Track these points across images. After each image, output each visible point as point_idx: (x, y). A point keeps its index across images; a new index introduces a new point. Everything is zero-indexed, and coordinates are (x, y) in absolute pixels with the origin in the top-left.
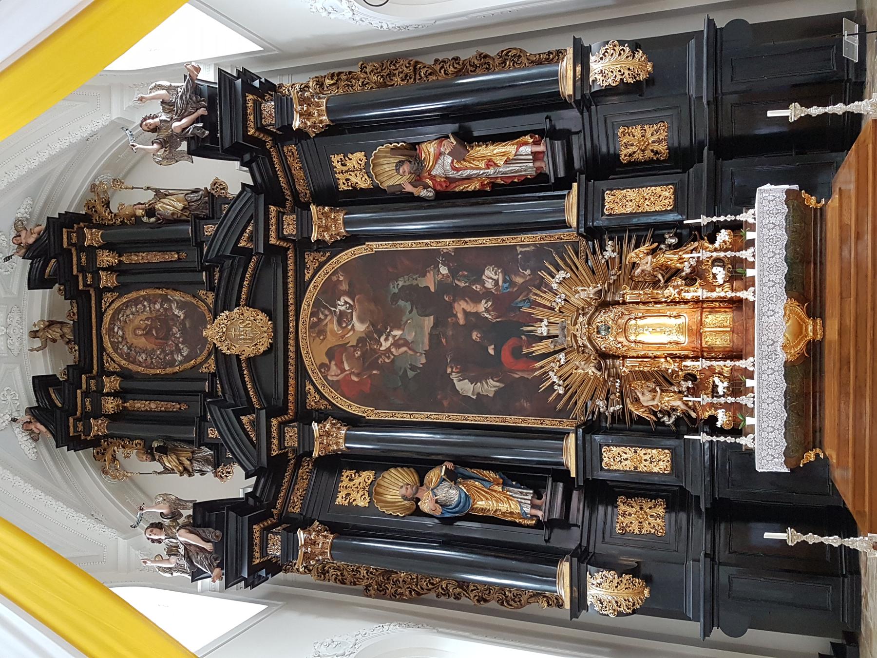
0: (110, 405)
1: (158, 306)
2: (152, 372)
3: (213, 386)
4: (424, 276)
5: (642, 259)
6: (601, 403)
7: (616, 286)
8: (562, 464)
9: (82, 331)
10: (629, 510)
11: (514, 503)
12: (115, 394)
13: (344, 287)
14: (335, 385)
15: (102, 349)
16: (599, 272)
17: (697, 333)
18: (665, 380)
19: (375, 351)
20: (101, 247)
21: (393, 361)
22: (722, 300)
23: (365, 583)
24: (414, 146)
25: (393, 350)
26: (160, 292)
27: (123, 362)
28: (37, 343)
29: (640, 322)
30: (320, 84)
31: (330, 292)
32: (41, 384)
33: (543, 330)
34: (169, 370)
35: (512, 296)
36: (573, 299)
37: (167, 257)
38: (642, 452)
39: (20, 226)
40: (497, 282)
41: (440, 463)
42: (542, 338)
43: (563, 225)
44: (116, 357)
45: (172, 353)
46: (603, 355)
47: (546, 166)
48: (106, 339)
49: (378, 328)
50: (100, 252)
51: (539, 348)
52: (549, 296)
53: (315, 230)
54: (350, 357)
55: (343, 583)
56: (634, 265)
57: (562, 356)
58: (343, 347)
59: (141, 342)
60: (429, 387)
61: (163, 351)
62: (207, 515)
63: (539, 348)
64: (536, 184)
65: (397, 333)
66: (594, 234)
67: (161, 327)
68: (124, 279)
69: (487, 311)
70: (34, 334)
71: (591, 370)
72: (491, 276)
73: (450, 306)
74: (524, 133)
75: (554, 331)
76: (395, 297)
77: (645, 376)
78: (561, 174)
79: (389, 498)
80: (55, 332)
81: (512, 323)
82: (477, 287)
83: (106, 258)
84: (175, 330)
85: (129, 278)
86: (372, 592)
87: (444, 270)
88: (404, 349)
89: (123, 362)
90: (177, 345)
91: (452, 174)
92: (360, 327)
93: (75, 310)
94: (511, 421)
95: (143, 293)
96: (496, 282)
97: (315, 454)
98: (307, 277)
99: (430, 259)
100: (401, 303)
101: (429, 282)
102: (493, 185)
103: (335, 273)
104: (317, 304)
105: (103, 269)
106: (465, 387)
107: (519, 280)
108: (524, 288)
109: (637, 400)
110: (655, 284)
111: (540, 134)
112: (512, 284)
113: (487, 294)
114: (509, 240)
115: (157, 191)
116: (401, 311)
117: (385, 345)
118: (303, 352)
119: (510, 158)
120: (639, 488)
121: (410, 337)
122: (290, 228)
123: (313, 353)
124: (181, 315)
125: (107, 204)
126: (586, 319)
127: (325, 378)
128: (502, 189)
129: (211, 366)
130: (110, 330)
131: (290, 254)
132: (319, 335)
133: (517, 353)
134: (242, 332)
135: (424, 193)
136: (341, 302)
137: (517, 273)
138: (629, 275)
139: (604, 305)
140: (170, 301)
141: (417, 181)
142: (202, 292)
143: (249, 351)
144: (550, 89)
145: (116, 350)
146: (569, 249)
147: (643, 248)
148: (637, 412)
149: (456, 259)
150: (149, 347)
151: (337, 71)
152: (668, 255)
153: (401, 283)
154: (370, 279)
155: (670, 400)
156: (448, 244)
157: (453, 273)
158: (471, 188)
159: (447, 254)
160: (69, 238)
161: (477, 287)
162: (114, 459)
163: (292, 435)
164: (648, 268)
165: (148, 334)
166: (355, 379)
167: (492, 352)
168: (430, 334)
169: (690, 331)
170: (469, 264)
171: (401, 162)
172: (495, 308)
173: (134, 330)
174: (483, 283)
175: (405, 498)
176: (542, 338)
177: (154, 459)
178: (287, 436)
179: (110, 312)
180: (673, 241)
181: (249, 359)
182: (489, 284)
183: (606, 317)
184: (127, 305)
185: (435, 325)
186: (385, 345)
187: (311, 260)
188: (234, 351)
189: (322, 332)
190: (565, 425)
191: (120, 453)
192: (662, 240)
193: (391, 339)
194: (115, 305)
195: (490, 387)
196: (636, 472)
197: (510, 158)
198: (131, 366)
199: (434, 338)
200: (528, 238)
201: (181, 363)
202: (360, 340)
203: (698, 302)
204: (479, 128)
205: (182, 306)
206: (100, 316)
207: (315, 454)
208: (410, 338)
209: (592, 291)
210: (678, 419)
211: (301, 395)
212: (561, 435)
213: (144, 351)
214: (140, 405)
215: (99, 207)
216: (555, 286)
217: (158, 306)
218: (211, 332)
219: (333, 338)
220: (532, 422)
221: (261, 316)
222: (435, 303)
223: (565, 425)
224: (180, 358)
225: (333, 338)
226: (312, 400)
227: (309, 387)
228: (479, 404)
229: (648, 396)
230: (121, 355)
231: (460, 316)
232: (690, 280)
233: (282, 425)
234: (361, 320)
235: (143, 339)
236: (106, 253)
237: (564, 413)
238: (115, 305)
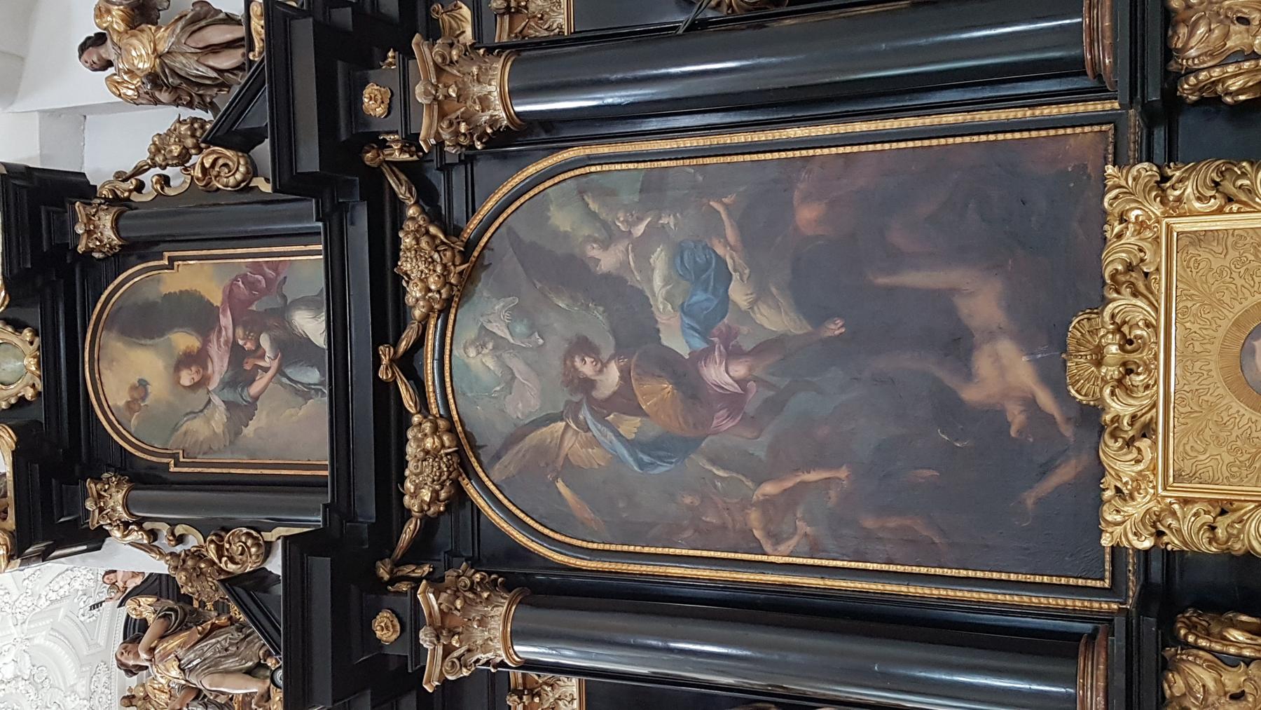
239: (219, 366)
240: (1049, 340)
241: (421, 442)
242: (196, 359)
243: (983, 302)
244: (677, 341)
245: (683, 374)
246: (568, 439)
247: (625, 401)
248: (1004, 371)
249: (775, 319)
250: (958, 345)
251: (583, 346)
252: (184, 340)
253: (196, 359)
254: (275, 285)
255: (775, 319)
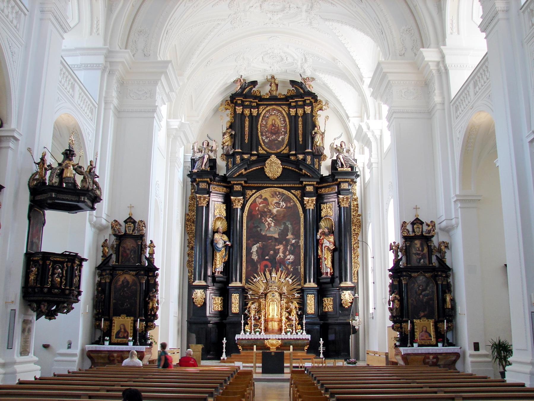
0: (247, 112)
1: (283, 130)
2: (259, 127)
3: (254, 155)
4: (292, 234)
5: (294, 305)
6: (251, 292)
7: (287, 298)
8: (232, 281)
9: (273, 99)
10: (219, 300)
11: (219, 267)
12: (251, 114)
13: (289, 205)
14: (255, 201)
15: (268, 105)
16: (291, 292)
17: (272, 320)
18: (259, 311)
19: (267, 216)
20: (304, 111)
21: (263, 223)
22: (281, 326)
23: (190, 214)
24: (333, 233)
25: (267, 223)
26: (288, 130)
27: (262, 115)
28: (269, 77)
29: (275, 305)
30: (356, 200)
31: (287, 200)
32: (254, 83)
33: (274, 275)
34: (259, 134)
35: (285, 265)
36: (283, 284)
37: (300, 136)
38: (238, 305)
39: (313, 79)
40: (289, 259)
41: (230, 241)
42: (271, 274)
43: (305, 282)
44: (264, 111)
45: (266, 135)
46: (266, 295)
47: (324, 276)
48: (271, 107)
49: (275, 218)
50: (302, 110)
51: (268, 274)
52: (284, 277)
53: (307, 198)
54: (264, 207)
55: (189, 206)
56: (292, 302)
57: (265, 281)
58: (268, 204)
59: (270, 122)
60: (255, 236)
61: (267, 131)
62: (212, 162)
63: (268, 274)
64: (318, 272)
65: (273, 224)
66: (302, 291)
67: (275, 131)
68: (293, 118)
69: (280, 256)
70: (273, 77)
71: (261, 291)
72: (291, 258)
73: (281, 243)
74: (334, 270)
75: (273, 279)
76: (285, 224)
77: (260, 305)
78: (321, 281)
79: (217, 222)
80: (274, 88)
81: (276, 264)
82: (287, 253)
83: (300, 112)
84: (274, 136)
85: (294, 119)
86: (188, 217)
87: (293, 241)
88: (267, 227)
89: (262, 115)
90: (268, 137)
91: (324, 245)
92: (275, 211)
93: (282, 97)
94: (244, 264)
95: (288, 123)
96: (289, 259)
97: (232, 198)
98: (292, 191)
99: (297, 237)
100: (283, 226)
101: (290, 236)
102: (320, 258)
103: (294, 202)
104: (283, 194)
105: (296, 110)
106: (255, 248)
107: (289, 267)
108: (287, 269)
109: (253, 303)
110: (287, 308)
111: (333, 275)
112: (288, 264)
113: (285, 256)
114: (302, 264)
115: (323, 133)
116: (280, 226)
117: (269, 220)
118: (266, 189)
119: (327, 266)
120: (226, 303)
121: (272, 229)
122: (309, 189)
123: (266, 193)
124: (280, 139)
125: (321, 109)
126: (276, 290)
127: (257, 197)
128: (318, 261)
129: (261, 152)
130: (274, 109)
131: (300, 185)
132: (272, 195)
133: (266, 266)
134: (274, 167)
135: (318, 236)
136: (284, 204)
137: (292, 266)
138: (289, 301)
139: (281, 295)
140: (285, 135)
141: (323, 234)
142: (288, 148)
143: (267, 170)
144: (343, 280)
145: (267, 111)
146: (299, 283)
147: (297, 306)
148: (249, 305)
149: (296, 246)
150: (268, 126)
151: (359, 206)
152: (295, 312)
153: (289, 226)
154: (290, 214)
155: (253, 313)
156: (302, 243)
157: (292, 245)
158: (319, 252)
159: (298, 242)
160: (308, 99)
161: (287, 253)
162: (227, 109)
163: (238, 188)
164: (291, 307)
165: (273, 125)
166: (257, 208)
167: (266, 258)
168: (272, 237)
169: (273, 318)
170: (295, 250)
171: (328, 229)
172: (281, 259)
173: (274, 119)
174: (289, 255)
175: (218, 228)
176: (271, 274)
177: (227, 129)
178: (237, 186)
179: (281, 109)
180: (299, 313)
181: (263, 168)
182: (288, 257)
183: (277, 295)
184: (284, 117)
185: (276, 239)
186: (269, 220)
187: (298, 193)
188: (267, 165)
189: (273, 196)
190: (244, 281)
191: (229, 112)
192: (299, 310)
193: (270, 222)
194: (283, 112)
195: (255, 257)
196: (231, 303)
197: (327, 266)
198: (261, 118)
199: (271, 237)
200: (302, 270)
201: (262, 139)
202: (270, 211)
203: (281, 320)
204: (337, 254)
205: (283, 139)
206: (279, 105)
207: (232, 198)
208: (271, 229)
209: (285, 291)
210: (247, 315)
211: (251, 188)
212: (241, 281)
213: (266, 123)
214: (247, 123)
215: (319, 106)
216: (287, 279)
217: (283, 130)
218: (273, 158)
219: (272, 200)
220: (244, 271)
221: (279, 174)
222: (282, 239)
223: (244, 281)
224: (264, 138)
225: (272, 200)
226: (249, 192)
227: (254, 191)
228: (249, 253)
229: (254, 307)
230: (265, 113)
231: (278, 247)
232: (287, 318)
233: (241, 184)
234: (277, 211)
235: (271, 123)
236: (303, 112)
237: (247, 282)
238: (283, 112)
239: (419, 252)
240: (424, 316)
241: (416, 274)
242: (419, 250)
243: (426, 313)
244: (423, 293)
245: (421, 294)
246: (416, 285)
247: (419, 289)
248: (422, 314)
249: (425, 300)
250: (424, 312)
251: (423, 286)
252: (420, 249)
253: (419, 250)
254: (426, 258)
255: (425, 300)
